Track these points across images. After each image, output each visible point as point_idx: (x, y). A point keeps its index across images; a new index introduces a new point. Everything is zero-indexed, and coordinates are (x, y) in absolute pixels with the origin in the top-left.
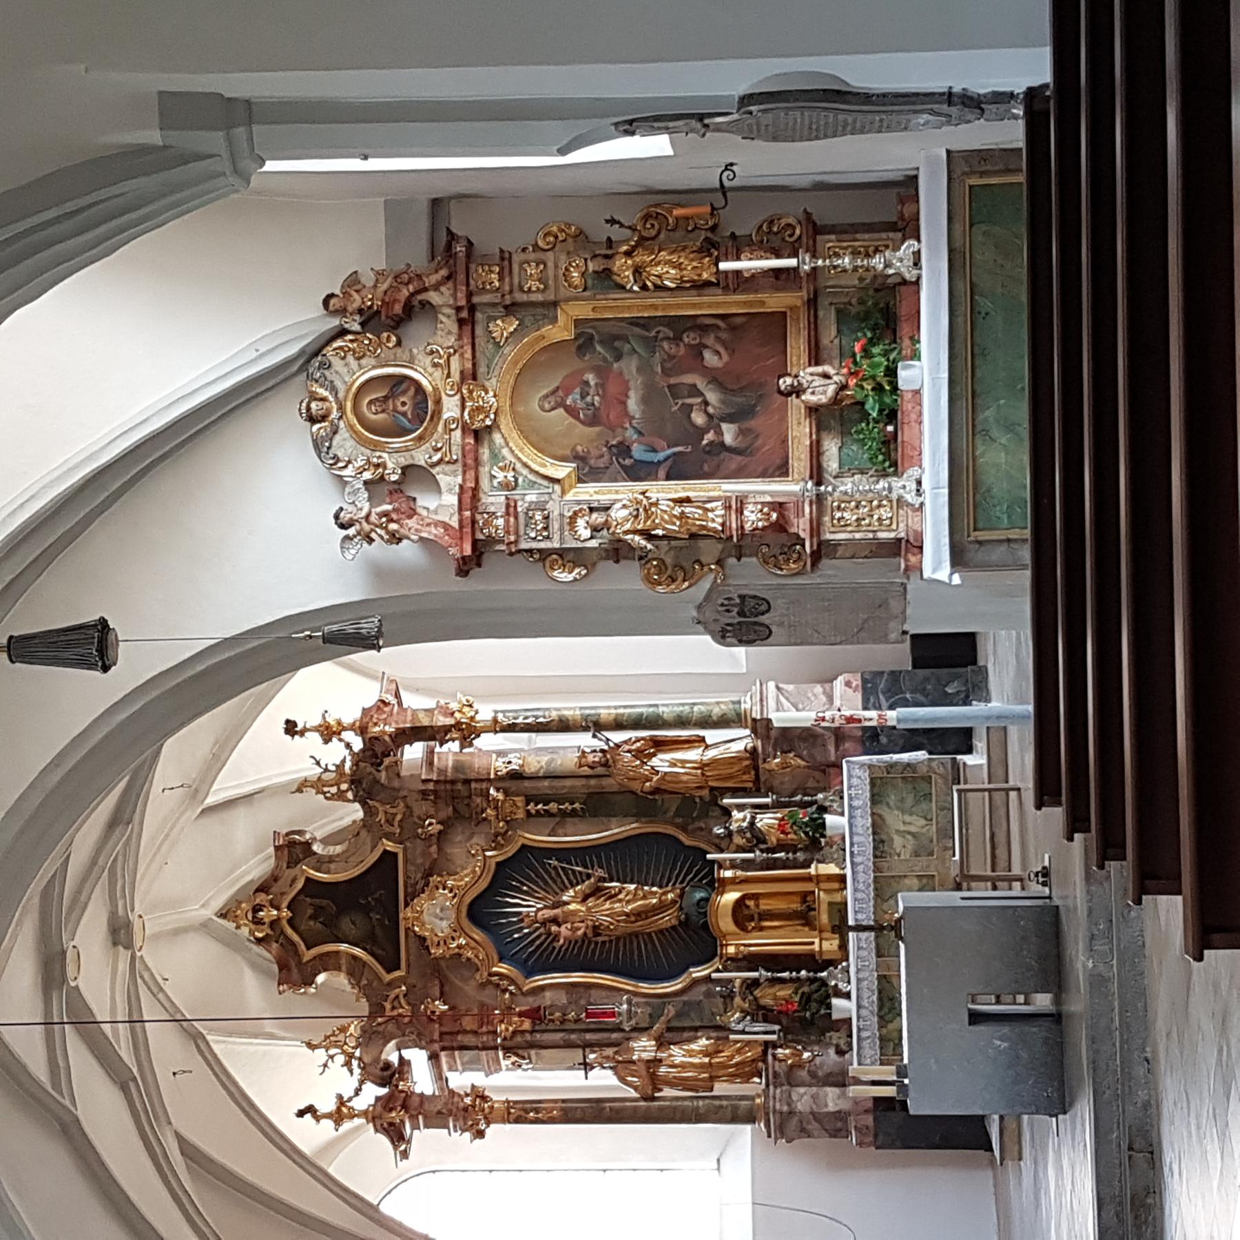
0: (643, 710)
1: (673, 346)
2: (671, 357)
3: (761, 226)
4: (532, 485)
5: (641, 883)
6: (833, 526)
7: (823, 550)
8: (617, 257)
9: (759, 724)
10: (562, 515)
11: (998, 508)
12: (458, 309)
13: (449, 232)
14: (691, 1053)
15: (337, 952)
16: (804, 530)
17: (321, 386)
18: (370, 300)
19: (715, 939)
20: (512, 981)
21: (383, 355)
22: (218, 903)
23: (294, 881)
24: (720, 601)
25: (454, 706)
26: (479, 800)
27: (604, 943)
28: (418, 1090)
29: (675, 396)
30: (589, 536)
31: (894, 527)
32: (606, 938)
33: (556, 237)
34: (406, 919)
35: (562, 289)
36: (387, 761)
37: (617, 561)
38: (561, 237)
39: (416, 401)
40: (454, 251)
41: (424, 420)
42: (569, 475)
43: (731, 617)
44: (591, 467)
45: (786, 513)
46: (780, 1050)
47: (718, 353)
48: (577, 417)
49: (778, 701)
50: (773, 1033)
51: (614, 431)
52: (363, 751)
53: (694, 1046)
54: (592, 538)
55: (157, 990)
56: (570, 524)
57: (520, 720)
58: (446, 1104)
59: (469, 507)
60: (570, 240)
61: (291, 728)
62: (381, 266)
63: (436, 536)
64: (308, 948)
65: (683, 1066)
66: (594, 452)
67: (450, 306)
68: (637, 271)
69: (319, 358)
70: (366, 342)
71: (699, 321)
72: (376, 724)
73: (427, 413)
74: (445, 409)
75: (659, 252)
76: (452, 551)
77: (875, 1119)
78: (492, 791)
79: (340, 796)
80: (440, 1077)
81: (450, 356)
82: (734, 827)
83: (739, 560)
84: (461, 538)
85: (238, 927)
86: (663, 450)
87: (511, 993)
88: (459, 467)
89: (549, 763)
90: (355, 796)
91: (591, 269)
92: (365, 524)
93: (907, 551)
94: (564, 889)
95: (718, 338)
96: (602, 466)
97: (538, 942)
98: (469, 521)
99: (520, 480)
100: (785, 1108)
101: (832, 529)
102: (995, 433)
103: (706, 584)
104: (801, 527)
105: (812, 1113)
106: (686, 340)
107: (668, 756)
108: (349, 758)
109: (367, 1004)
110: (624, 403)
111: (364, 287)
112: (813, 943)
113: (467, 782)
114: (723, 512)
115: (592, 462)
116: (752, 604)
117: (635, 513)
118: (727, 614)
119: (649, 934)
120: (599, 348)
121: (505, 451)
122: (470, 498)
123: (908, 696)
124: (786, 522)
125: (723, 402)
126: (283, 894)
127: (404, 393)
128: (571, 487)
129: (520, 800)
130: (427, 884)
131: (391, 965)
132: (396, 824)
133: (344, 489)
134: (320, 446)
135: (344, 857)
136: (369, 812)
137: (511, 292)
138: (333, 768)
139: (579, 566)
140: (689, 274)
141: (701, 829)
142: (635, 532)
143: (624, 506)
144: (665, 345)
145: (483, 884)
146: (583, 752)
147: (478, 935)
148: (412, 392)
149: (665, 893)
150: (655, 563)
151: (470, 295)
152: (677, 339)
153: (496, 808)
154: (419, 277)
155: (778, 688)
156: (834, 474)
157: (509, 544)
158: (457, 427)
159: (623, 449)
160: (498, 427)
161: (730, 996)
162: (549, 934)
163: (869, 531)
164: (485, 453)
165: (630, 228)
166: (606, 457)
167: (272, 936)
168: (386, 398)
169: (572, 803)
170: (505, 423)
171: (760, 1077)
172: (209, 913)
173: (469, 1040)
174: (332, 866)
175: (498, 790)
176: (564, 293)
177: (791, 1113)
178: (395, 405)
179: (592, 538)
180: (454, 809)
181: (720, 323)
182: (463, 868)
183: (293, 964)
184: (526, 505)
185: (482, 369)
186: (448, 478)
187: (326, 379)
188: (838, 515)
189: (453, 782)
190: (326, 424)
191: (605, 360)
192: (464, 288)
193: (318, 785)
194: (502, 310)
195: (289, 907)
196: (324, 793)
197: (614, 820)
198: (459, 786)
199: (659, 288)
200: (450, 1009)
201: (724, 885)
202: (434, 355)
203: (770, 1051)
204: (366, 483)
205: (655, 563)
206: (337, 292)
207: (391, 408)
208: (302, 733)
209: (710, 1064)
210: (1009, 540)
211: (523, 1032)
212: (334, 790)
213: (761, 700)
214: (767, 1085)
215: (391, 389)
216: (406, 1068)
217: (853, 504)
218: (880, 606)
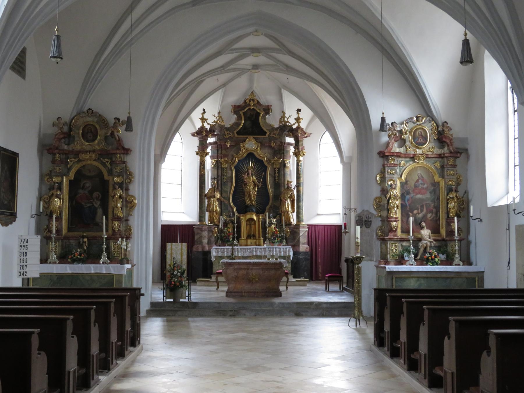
0: (302, 198)
4: (400, 171)
5: (258, 196)
7: (383, 240)
9: (298, 226)
10: (393, 178)
12: (444, 154)
13: (462, 153)
14: (216, 207)
15: (241, 120)
17: (425, 120)
19: (245, 213)
20: (233, 163)
22: (256, 91)
23: (259, 110)
24: (370, 216)
25: (304, 151)
26: (279, 156)
27: (242, 186)
28: (209, 139)
32: (243, 186)
33: (459, 179)
34: (250, 137)
36: (291, 134)
38: (459, 180)
42: (402, 180)
46: (216, 228)
47: (431, 217)
48: (416, 182)
49: (303, 231)
50: (221, 227)
52: (293, 128)
53: (218, 208)
54: (388, 185)
55: (239, 76)
56: (391, 179)
57: (300, 167)
58: (205, 145)
60: (458, 182)
61: (299, 110)
62: (454, 136)
64: (243, 113)
65: (213, 205)
68: (453, 198)
71: (438, 213)
72: (301, 131)
76: (386, 150)
77: (200, 252)
78: (281, 159)
79: (281, 122)
80: (211, 144)
82: (272, 219)
83: (381, 221)
85: (249, 96)
87: (230, 163)
88: (405, 153)
89: (288, 174)
90: (281, 126)
91: (453, 187)
92: (393, 129)
94: (256, 177)
95: (434, 217)
97: (242, 170)
100: (203, 230)
102: (418, 283)
103: (375, 212)
104: (391, 236)
105: (202, 236)
106: (434, 209)
107: (290, 203)
108: (291, 124)
109: (228, 127)
110: (419, 193)
112: (243, 238)
113: (284, 153)
115: (405, 185)
119: (244, 197)
120: (432, 188)
121: (408, 164)
122: (399, 155)
123: (304, 263)
126: (257, 107)
127: (423, 140)
128: (399, 180)
129: (279, 166)
130: (259, 143)
131: (239, 133)
132: (273, 136)
134: (410, 120)
135: (265, 123)
136: (277, 129)
137: (447, 167)
138: (288, 120)
139: (380, 181)
140: (452, 210)
141: (270, 211)
142: (390, 195)
143: (396, 193)
144: (433, 204)
145: (257, 156)
146: (291, 183)
147: (245, 155)
148: (423, 142)
149: (254, 202)
151: (447, 157)
152: (434, 207)
153: (277, 160)
154: (452, 145)
155: (306, 231)
157: (387, 164)
159: (408, 193)
160: (414, 163)
161: (230, 217)
162: (245, 173)
164: (408, 159)
165: (463, 196)
166: (406, 189)
167: (246, 104)
168: (422, 135)
169: (278, 179)
171: (210, 224)
172: (254, 89)
173: (220, 152)
174: (263, 120)
175: (281, 161)
176: (446, 180)
177: (202, 231)
180: (277, 150)
181: (438, 218)
182: (262, 152)
183: (239, 109)
185: (428, 159)
186: (402, 150)
188: (394, 245)
189: (284, 150)
193: (283, 117)
195: (253, 109)
196: (282, 118)
197: (273, 190)
198: (282, 151)
199: (448, 204)
200: (227, 147)
201: (258, 216)
203: (216, 226)
206: (448, 125)
208: (298, 113)
209: (213, 211)
211: (221, 165)
212: (282, 120)
213: (304, 227)
214: (208, 225)
216: (214, 136)
218: (367, 255)
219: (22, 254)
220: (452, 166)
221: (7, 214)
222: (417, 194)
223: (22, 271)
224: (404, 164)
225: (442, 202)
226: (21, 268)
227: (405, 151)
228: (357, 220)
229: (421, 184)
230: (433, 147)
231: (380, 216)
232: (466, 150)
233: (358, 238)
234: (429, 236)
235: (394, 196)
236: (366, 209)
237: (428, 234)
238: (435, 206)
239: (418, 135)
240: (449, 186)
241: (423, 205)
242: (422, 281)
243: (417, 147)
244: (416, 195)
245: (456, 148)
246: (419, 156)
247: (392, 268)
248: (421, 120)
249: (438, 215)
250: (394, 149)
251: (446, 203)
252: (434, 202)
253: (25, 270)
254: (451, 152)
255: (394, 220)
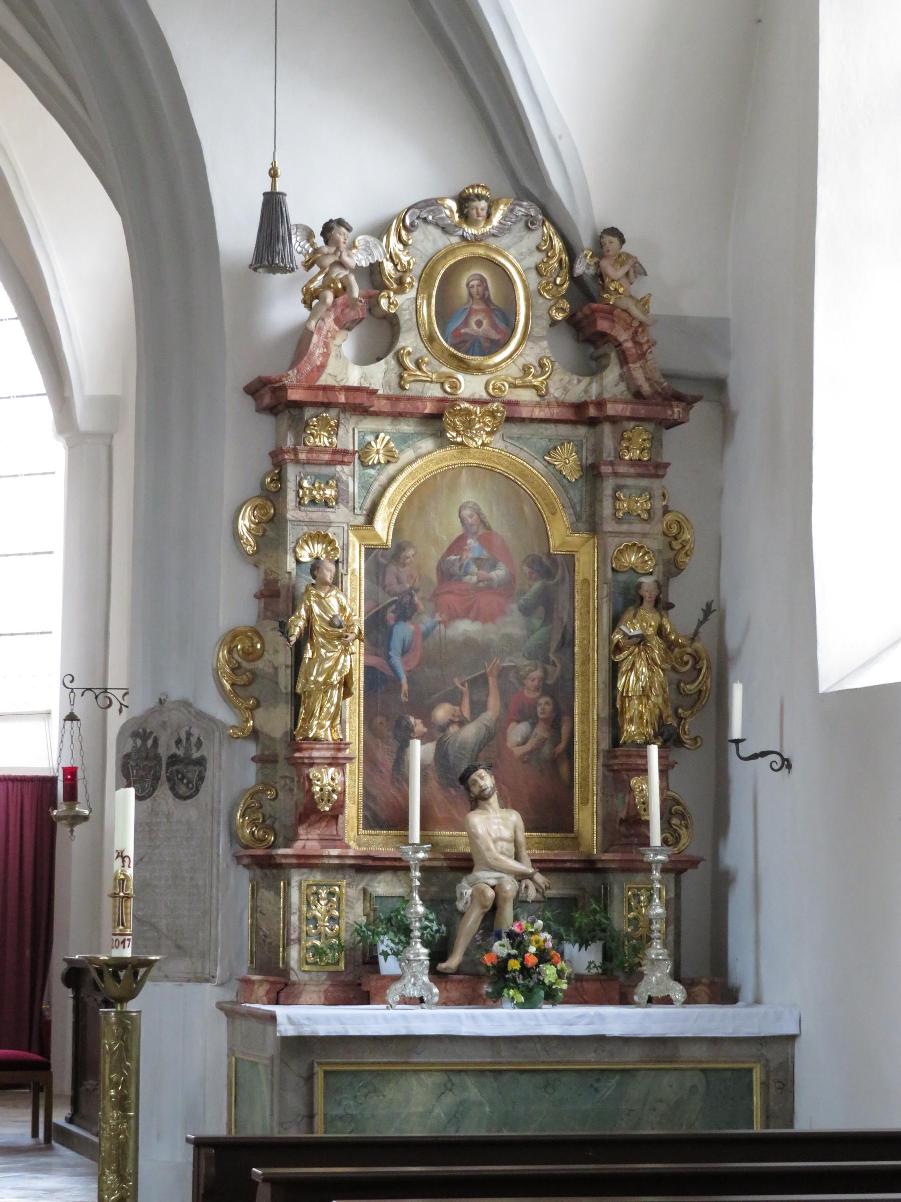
1: (536, 682)
2: (521, 680)
3: (678, 803)
4: (366, 487)
6: (309, 886)
8: (657, 616)
10: (329, 524)
11: (352, 1103)
12: (600, 404)
13: (696, 399)
16: (304, 847)
17: (504, 217)
18: (616, 290)
21: (541, 300)
24: (196, 732)
29: (473, 683)
30: (302, 560)
31: (306, 968)
33: (675, 538)
35: (617, 540)
37: (259, 596)
38: (676, 545)
39: (482, 340)
40: (674, 403)
41: (458, 349)
42: (377, 537)
43: (168, 747)
44: (386, 566)
45: (324, 824)
47: (524, 742)
48: (450, 551)
51: (430, 600)
54: (298, 562)
56: (318, 534)
59: (351, 401)
60: (671, 555)
62: (655, 308)
63: (313, 354)
66: (404, 572)
67: (600, 394)
68: (641, 640)
69: (540, 217)
70: (558, 282)
71: (565, 718)
73: (466, 353)
74: (468, 377)
75: (663, 670)
76: (293, 373)
81: (535, 387)
83: (253, 759)
84: (310, 388)
86: (405, 663)
88: (395, 391)
91: (643, 580)
93: (272, 983)
95: (542, 742)
96: (387, 582)
98: (332, 400)
99: (372, 472)
101: (304, 885)
102: (449, 1099)
106: (542, 700)
110: (466, 613)
111: (631, 284)
114: (330, 739)
115: (392, 569)
116: (190, 775)
117: (337, 623)
118: (175, 738)
120: (536, 586)
121: (409, 455)
124: (310, 826)
125: (462, 746)
127: (494, 325)
128: (361, 539)
133: (366, 234)
137: (615, 474)
139: (257, 544)
140: (634, 707)
142: (309, 620)
143: (343, 609)
144: (537, 673)
148: (494, 335)
150: (259, 646)
151: (614, 420)
152: (545, 689)
154: (642, 356)
156: (370, 890)
157: (295, 451)
158: (446, 391)
159: (406, 611)
160: (441, 447)
163: (300, 933)
164: (407, 427)
165: (696, 633)
166: (397, 588)
168: (485, 300)
170: (447, 457)
176: (613, 543)
178: (477, 311)
179: (298, 562)
181: (562, 746)
184: (344, 477)
187: (514, 223)
188: (323, 894)
190: (457, 219)
191: (523, 593)
192: (628, 414)
194: (589, 462)
199: (614, 670)
202: (538, 369)
204: (379, 265)
205: (259, 646)
206: (626, 248)
207: (475, 307)
210: (311, 1116)
215: (499, 309)
217: (336, 913)
218: (178, 947)
220: (640, 470)
222: (454, 615)
224: (389, 451)
225: (586, 660)
227: (394, 380)
228: (127, 756)
229: (478, 561)
230: (542, 366)
231: (255, 734)
232: (719, 385)
233: (122, 856)
234: (511, 847)
235: (331, 623)
236: (175, 695)
237: (507, 834)
238: (550, 682)
239: (464, 292)
240: (622, 578)
241: (484, 678)
242: (472, 1091)
243: (460, 360)
244: (446, 623)
245: (666, 376)
246: (468, 412)
247: (308, 1018)
248: (484, 213)
249: (564, 730)
250: (333, 366)
251: (605, 666)
252: (546, 660)
254: (638, 395)
255: (328, 754)
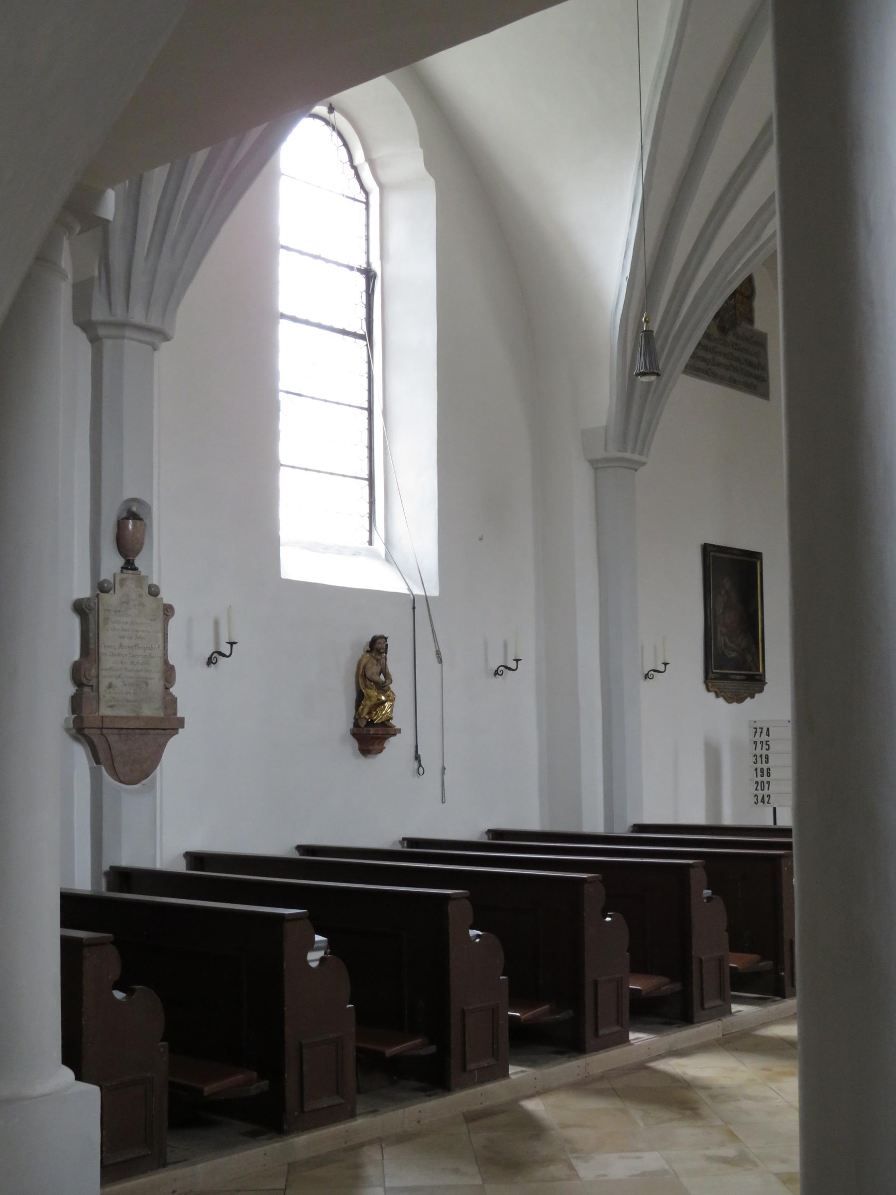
219: (759, 759)
221: (738, 677)
223: (760, 793)
226: (759, 788)
253: (766, 792)
